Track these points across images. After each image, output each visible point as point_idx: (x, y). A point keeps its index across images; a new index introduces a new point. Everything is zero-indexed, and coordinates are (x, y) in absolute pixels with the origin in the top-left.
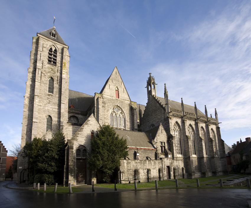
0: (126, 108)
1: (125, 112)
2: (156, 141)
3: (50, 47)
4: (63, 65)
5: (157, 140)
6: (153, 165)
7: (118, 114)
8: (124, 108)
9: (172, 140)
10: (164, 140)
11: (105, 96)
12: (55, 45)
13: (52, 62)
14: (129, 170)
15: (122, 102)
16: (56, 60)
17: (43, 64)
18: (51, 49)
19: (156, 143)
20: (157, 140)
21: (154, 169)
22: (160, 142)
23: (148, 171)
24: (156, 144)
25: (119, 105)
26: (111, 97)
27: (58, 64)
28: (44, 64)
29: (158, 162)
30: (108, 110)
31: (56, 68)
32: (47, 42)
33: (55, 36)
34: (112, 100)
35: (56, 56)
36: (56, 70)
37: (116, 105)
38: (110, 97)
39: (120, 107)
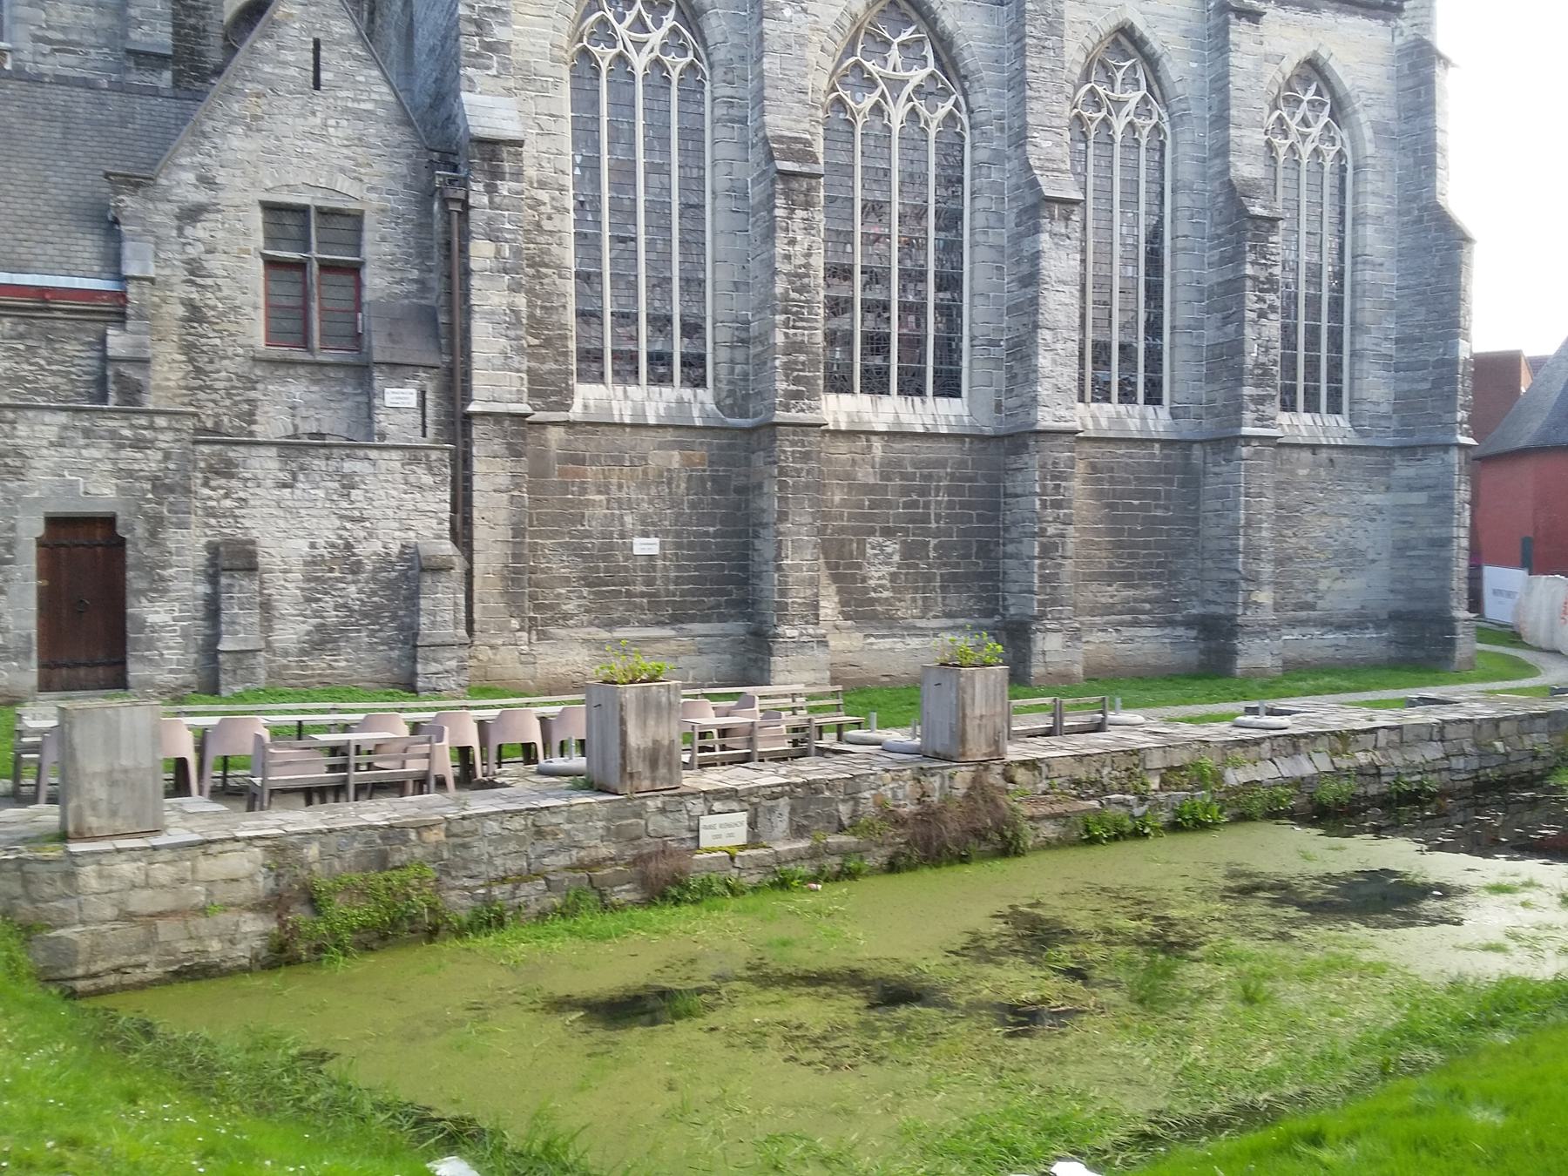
2: (201, 196)
5: (222, 177)
10: (344, 184)
19: (192, 214)
22: (269, 208)
24: (199, 231)
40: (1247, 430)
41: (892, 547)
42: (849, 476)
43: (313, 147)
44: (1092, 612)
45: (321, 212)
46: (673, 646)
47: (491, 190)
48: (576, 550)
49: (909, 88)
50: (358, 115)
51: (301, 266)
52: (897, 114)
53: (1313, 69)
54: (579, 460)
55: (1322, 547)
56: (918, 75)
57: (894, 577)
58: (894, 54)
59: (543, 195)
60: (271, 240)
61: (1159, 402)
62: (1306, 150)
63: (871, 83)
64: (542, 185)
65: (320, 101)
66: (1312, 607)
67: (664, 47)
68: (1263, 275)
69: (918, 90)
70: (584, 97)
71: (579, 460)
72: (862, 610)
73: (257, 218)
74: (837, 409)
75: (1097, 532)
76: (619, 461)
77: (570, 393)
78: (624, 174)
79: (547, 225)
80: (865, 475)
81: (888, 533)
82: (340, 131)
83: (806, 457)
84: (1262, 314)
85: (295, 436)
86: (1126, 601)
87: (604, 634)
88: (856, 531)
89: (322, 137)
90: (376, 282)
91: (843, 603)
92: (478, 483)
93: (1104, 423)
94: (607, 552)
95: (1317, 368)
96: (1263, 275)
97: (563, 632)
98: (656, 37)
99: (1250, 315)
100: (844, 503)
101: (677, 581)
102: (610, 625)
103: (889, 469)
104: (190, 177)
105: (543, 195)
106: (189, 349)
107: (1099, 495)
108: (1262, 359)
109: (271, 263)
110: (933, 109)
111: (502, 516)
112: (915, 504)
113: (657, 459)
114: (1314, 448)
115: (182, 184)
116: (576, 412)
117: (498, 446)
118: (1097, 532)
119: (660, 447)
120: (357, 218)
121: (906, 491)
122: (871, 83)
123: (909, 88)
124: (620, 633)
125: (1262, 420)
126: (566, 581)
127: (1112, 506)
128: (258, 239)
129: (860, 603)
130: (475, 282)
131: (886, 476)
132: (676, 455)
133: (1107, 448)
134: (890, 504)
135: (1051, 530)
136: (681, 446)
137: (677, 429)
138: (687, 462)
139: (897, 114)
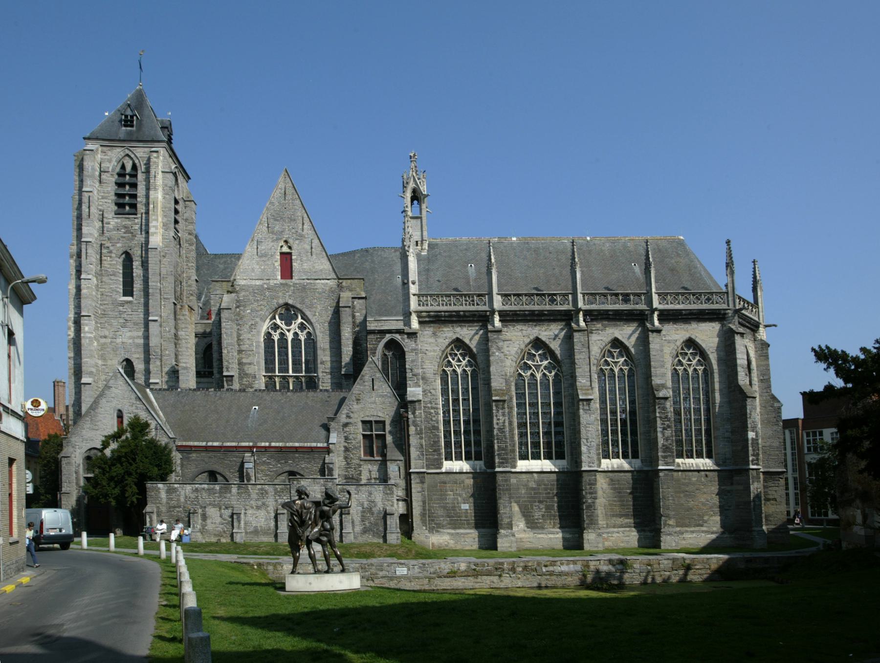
1: (313, 320)
2: (348, 420)
3: (120, 164)
4: (151, 206)
5: (352, 415)
7: (292, 332)
8: (311, 307)
9: (407, 412)
10: (380, 414)
11: (243, 282)
12: (130, 153)
13: (127, 208)
17: (102, 221)
18: (123, 167)
19: (346, 425)
20: (348, 417)
21: (258, 508)
22: (364, 422)
24: (347, 429)
25: (290, 302)
27: (141, 208)
28: (105, 220)
29: (276, 489)
30: (253, 326)
31: (136, 221)
32: (109, 153)
33: (132, 121)
34: (268, 289)
35: (134, 186)
36: (137, 227)
37: (281, 302)
39: (298, 306)
40: (660, 467)
41: (542, 506)
42: (526, 485)
43: (373, 406)
44: (614, 527)
45: (376, 422)
48: (445, 508)
49: (542, 368)
51: (372, 435)
52: (539, 376)
53: (690, 343)
55: (704, 504)
56: (545, 363)
57: (543, 516)
58: (538, 358)
59: (432, 411)
60: (364, 430)
61: (638, 458)
62: (690, 371)
63: (530, 368)
64: (432, 408)
65: (374, 394)
66: (702, 526)
68: (663, 416)
69: (545, 368)
70: (444, 381)
72: (532, 524)
73: (360, 425)
74: (523, 465)
75: (615, 501)
77: (442, 464)
78: (456, 401)
80: (532, 484)
81: (540, 502)
83: (506, 481)
84: (664, 429)
86: (626, 523)
88: (529, 502)
89: (375, 403)
91: (527, 523)
92: (413, 490)
93: (615, 466)
94: (454, 508)
95: (702, 443)
96: (663, 416)
99: (659, 430)
100: (525, 493)
103: (539, 483)
104: (344, 416)
105: (432, 411)
106: (346, 458)
107: (614, 489)
108: (666, 443)
109: (364, 435)
110: (550, 372)
111: (420, 499)
112: (549, 493)
114: (699, 471)
116: (443, 470)
117: (418, 480)
118: (615, 501)
121: (546, 489)
122: (530, 368)
123: (542, 368)
125: (667, 464)
127: (619, 493)
128: (361, 430)
129: (533, 523)
130: (411, 437)
131: (539, 485)
133: (616, 474)
134: (540, 493)
135: (590, 501)
139: (539, 376)
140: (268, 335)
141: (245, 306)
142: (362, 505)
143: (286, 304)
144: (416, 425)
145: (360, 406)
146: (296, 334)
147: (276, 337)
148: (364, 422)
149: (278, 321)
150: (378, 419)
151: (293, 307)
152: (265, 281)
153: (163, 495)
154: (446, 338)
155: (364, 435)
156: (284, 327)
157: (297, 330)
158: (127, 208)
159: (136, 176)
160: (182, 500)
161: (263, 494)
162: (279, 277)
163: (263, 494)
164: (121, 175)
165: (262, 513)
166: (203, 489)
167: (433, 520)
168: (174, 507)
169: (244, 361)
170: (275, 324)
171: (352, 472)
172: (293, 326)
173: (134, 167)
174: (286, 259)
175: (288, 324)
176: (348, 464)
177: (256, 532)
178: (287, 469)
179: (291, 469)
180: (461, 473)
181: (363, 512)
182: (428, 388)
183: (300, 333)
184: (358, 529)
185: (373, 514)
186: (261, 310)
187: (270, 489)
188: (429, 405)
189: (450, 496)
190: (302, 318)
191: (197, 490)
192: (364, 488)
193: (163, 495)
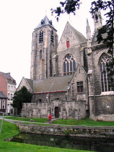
0: (76, 53)
6: (43, 106)
14: (27, 109)
15: (72, 49)
16: (43, 38)
19: (73, 84)
20: (73, 81)
21: (44, 109)
22: (77, 82)
23: (39, 110)
25: (69, 53)
26: (63, 49)
37: (67, 54)
38: (62, 50)
43: (80, 77)
46: (111, 117)
47: (89, 78)
48: (101, 107)
50: (82, 74)
54: (102, 99)
59: (97, 76)
64: (97, 76)
67: (107, 61)
71: (102, 99)
73: (76, 83)
76: (105, 99)
79: (98, 79)
82: (81, 75)
85: (79, 99)
87: (104, 115)
90: (84, 87)
92: (90, 102)
94: (104, 107)
97: (101, 115)
98: (107, 60)
101: (111, 110)
102: (105, 114)
104: (72, 81)
105: (97, 76)
106: (73, 93)
109: (77, 86)
111: (92, 105)
113: (108, 98)
115: (72, 82)
116: (101, 95)
117: (91, 99)
119: (109, 97)
120: (83, 82)
124: (106, 115)
126: (101, 110)
128: (76, 85)
132: (110, 98)
136: (111, 97)
137: (110, 95)
138: (112, 99)
140: (64, 62)
141: (59, 57)
142: (69, 107)
143: (68, 54)
144: (90, 82)
145: (77, 78)
146: (71, 61)
147: (66, 63)
148: (77, 82)
149: (66, 59)
150: (81, 81)
151: (70, 54)
152: (63, 49)
153: (25, 106)
154: (100, 53)
155: (77, 86)
156: (68, 60)
157: (71, 60)
158: (41, 41)
159: (43, 34)
160: (29, 107)
161: (45, 105)
162: (66, 48)
163: (45, 105)
164: (41, 34)
165: (44, 110)
166: (33, 104)
167: (98, 112)
168: (27, 109)
169: (59, 70)
170: (66, 60)
171: (74, 97)
172: (70, 59)
173: (43, 32)
174: (68, 42)
175: (69, 59)
176: (73, 95)
177: (43, 116)
178: (57, 98)
179: (58, 98)
180: (106, 95)
181: (69, 110)
182: (96, 70)
183: (72, 61)
184: (68, 115)
185: (72, 110)
186: (63, 57)
187: (47, 104)
188: (96, 75)
189: (103, 103)
190: (72, 57)
191: (31, 105)
192: (69, 102)
193: (25, 106)
